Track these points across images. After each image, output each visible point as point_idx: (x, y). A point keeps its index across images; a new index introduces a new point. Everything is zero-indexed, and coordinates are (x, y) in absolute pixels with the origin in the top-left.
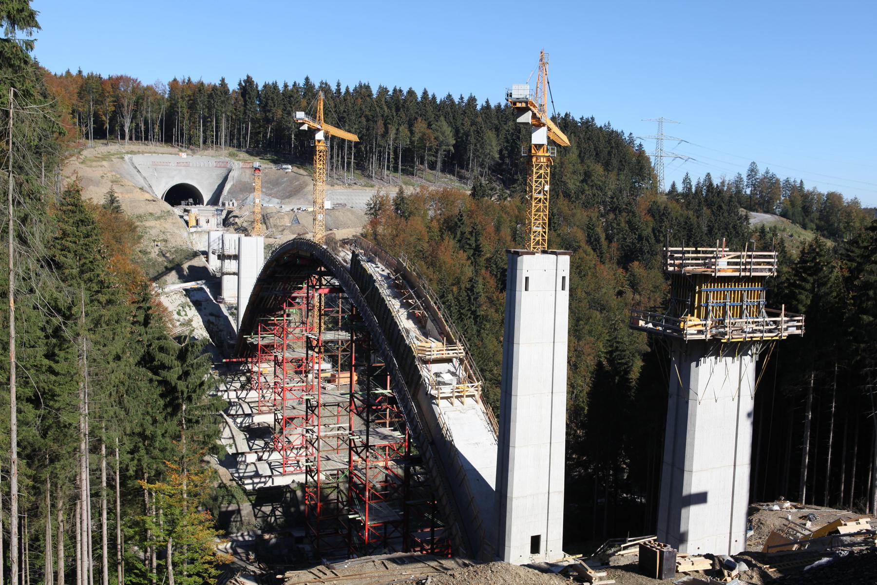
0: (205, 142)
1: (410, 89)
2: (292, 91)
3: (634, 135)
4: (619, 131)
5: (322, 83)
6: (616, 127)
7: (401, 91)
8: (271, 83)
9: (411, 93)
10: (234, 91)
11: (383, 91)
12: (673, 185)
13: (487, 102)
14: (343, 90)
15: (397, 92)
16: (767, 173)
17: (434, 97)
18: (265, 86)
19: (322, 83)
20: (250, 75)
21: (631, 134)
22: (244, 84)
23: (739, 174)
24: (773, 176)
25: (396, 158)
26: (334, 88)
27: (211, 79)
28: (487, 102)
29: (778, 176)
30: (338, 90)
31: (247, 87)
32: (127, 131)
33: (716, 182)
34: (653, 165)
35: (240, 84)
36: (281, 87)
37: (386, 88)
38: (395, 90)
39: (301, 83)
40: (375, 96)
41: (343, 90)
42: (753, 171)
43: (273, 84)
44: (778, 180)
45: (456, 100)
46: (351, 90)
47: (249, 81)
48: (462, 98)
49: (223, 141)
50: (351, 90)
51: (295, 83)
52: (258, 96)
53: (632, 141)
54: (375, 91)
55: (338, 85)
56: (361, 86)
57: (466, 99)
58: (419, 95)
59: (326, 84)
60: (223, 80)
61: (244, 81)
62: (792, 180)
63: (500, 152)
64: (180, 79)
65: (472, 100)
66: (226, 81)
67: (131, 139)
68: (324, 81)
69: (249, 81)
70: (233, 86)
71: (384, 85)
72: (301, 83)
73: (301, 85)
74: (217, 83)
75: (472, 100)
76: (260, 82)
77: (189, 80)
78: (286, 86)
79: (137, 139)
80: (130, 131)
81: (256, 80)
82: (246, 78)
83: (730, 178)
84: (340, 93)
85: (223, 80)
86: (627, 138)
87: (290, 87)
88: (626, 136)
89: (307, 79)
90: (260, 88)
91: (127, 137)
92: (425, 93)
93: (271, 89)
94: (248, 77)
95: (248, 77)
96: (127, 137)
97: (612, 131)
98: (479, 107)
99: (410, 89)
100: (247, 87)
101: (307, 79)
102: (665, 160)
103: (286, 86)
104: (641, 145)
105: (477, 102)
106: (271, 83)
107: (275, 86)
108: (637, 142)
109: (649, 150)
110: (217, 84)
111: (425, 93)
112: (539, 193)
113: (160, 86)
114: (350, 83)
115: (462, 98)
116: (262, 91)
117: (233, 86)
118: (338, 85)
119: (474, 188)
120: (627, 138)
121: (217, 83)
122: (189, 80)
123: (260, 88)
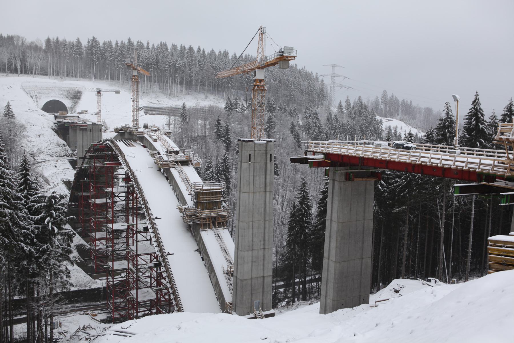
1: (190, 46)
5: (138, 42)
6: (308, 69)
7: (185, 47)
8: (107, 41)
9: (191, 48)
11: (174, 47)
12: (340, 102)
13: (235, 54)
15: (183, 48)
17: (204, 52)
19: (138, 42)
20: (95, 37)
21: (317, 74)
23: (377, 96)
24: (396, 98)
26: (145, 45)
27: (71, 38)
28: (235, 54)
29: (398, 98)
30: (148, 46)
32: (19, 68)
33: (364, 101)
34: (329, 91)
35: (89, 42)
36: (114, 44)
37: (176, 46)
38: (181, 46)
40: (169, 51)
41: (151, 47)
43: (109, 42)
44: (398, 101)
45: (217, 53)
46: (156, 47)
47: (94, 40)
48: (220, 52)
49: (78, 75)
50: (156, 47)
51: (122, 41)
54: (169, 47)
55: (148, 43)
57: (222, 52)
58: (196, 50)
59: (141, 42)
60: (78, 39)
64: (51, 38)
65: (226, 54)
66: (80, 40)
68: (140, 41)
69: (94, 40)
70: (84, 43)
71: (175, 43)
72: (126, 42)
74: (74, 40)
75: (226, 54)
77: (57, 39)
78: (117, 43)
82: (92, 38)
83: (372, 99)
85: (78, 39)
86: (315, 77)
90: (101, 44)
92: (199, 49)
94: (94, 38)
95: (94, 38)
98: (230, 58)
99: (190, 46)
102: (337, 88)
103: (117, 43)
105: (229, 55)
106: (107, 41)
107: (110, 43)
108: (320, 79)
109: (327, 82)
111: (199, 49)
115: (220, 52)
117: (84, 43)
118: (148, 43)
121: (75, 41)
122: (57, 39)
123: (101, 44)
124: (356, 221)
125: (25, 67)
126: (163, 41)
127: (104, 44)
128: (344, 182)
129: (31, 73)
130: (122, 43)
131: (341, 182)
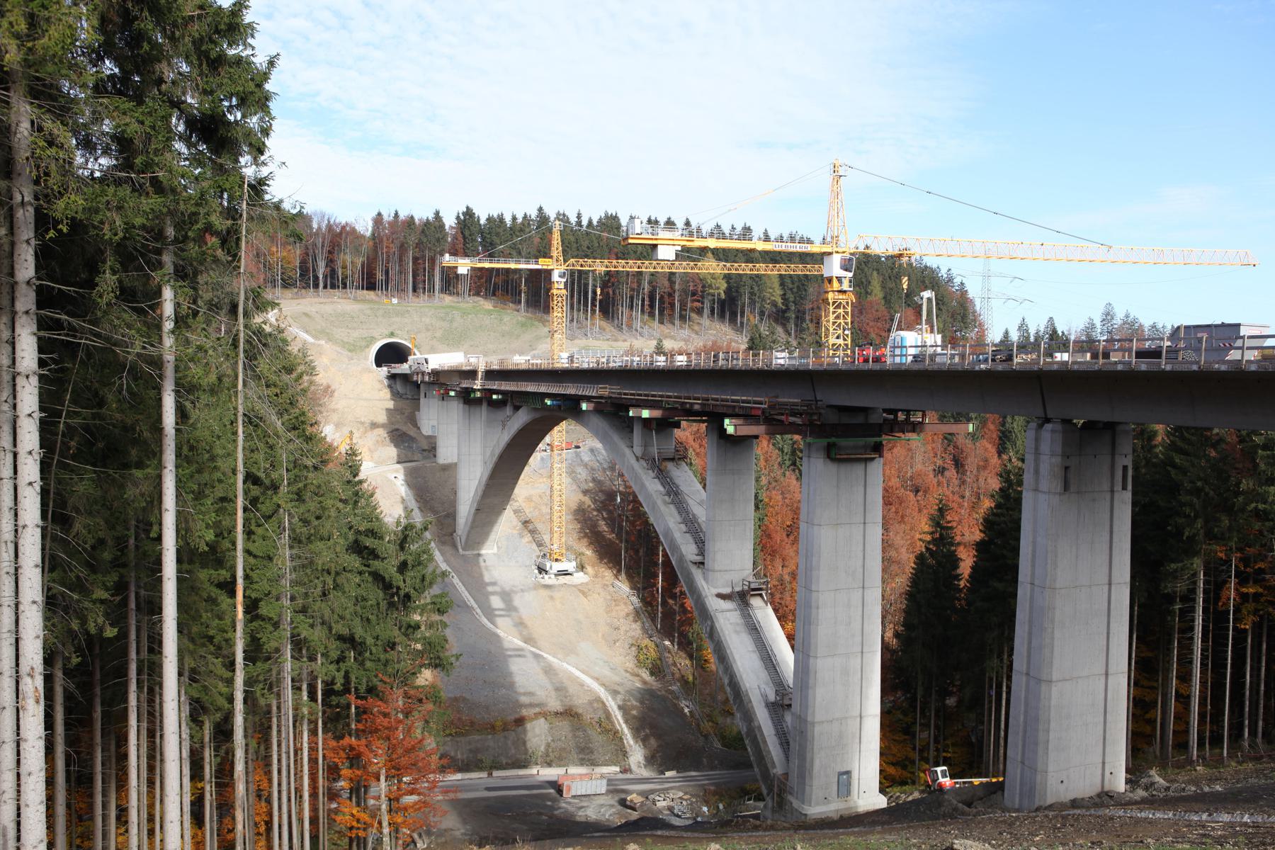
0: (415, 290)
2: (522, 224)
3: (954, 272)
4: (934, 266)
5: (558, 214)
8: (495, 216)
10: (451, 227)
12: (1007, 333)
14: (585, 223)
16: (1127, 316)
18: (489, 219)
20: (470, 206)
22: (462, 217)
24: (1135, 321)
25: (652, 306)
26: (573, 220)
27: (422, 213)
30: (579, 223)
31: (467, 219)
34: (978, 308)
35: (458, 218)
39: (533, 214)
41: (585, 223)
42: (1108, 316)
44: (1141, 326)
46: (595, 223)
47: (469, 213)
49: (437, 287)
50: (595, 223)
52: (482, 232)
53: (950, 280)
55: (579, 216)
56: (607, 216)
59: (564, 215)
60: (437, 213)
61: (463, 213)
62: (1160, 326)
63: (784, 296)
67: (325, 287)
69: (469, 213)
70: (449, 221)
72: (533, 214)
73: (533, 217)
76: (482, 215)
78: (514, 218)
79: (333, 287)
80: (325, 277)
81: (477, 212)
84: (581, 226)
85: (437, 213)
86: (945, 276)
87: (520, 220)
88: (943, 273)
89: (540, 209)
90: (483, 221)
91: (321, 285)
93: (496, 223)
94: (468, 208)
95: (468, 208)
96: (321, 285)
97: (926, 267)
100: (467, 219)
101: (540, 209)
103: (514, 218)
104: (962, 284)
106: (495, 216)
107: (501, 219)
108: (957, 281)
110: (430, 218)
112: (838, 338)
113: (362, 221)
114: (593, 213)
115: (733, 228)
116: (485, 225)
117: (449, 221)
118: (579, 216)
119: (752, 340)
120: (945, 276)
121: (431, 216)
123: (483, 221)
124: (1090, 586)
125: (333, 273)
126: (611, 211)
127: (487, 219)
128: (1060, 494)
129: (345, 287)
130: (525, 217)
131: (1055, 493)
